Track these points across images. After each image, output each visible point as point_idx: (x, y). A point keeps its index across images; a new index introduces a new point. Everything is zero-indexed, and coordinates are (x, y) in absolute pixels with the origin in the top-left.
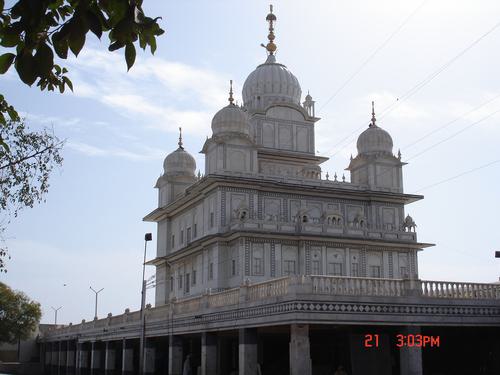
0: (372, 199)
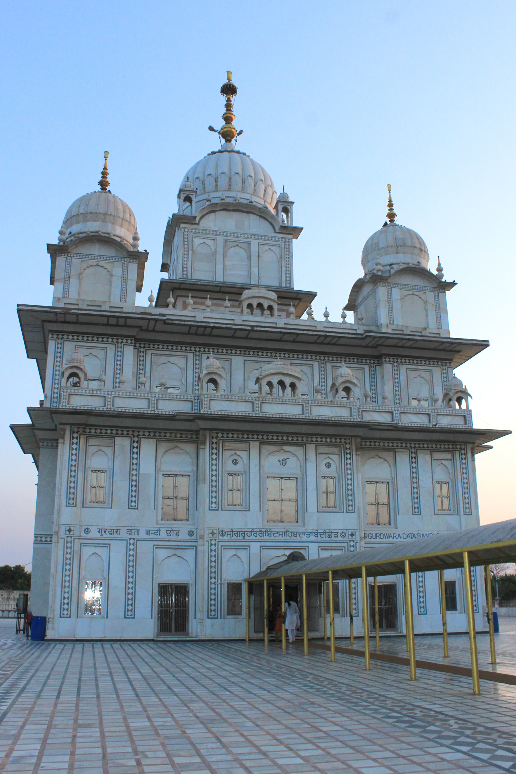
0: (385, 351)
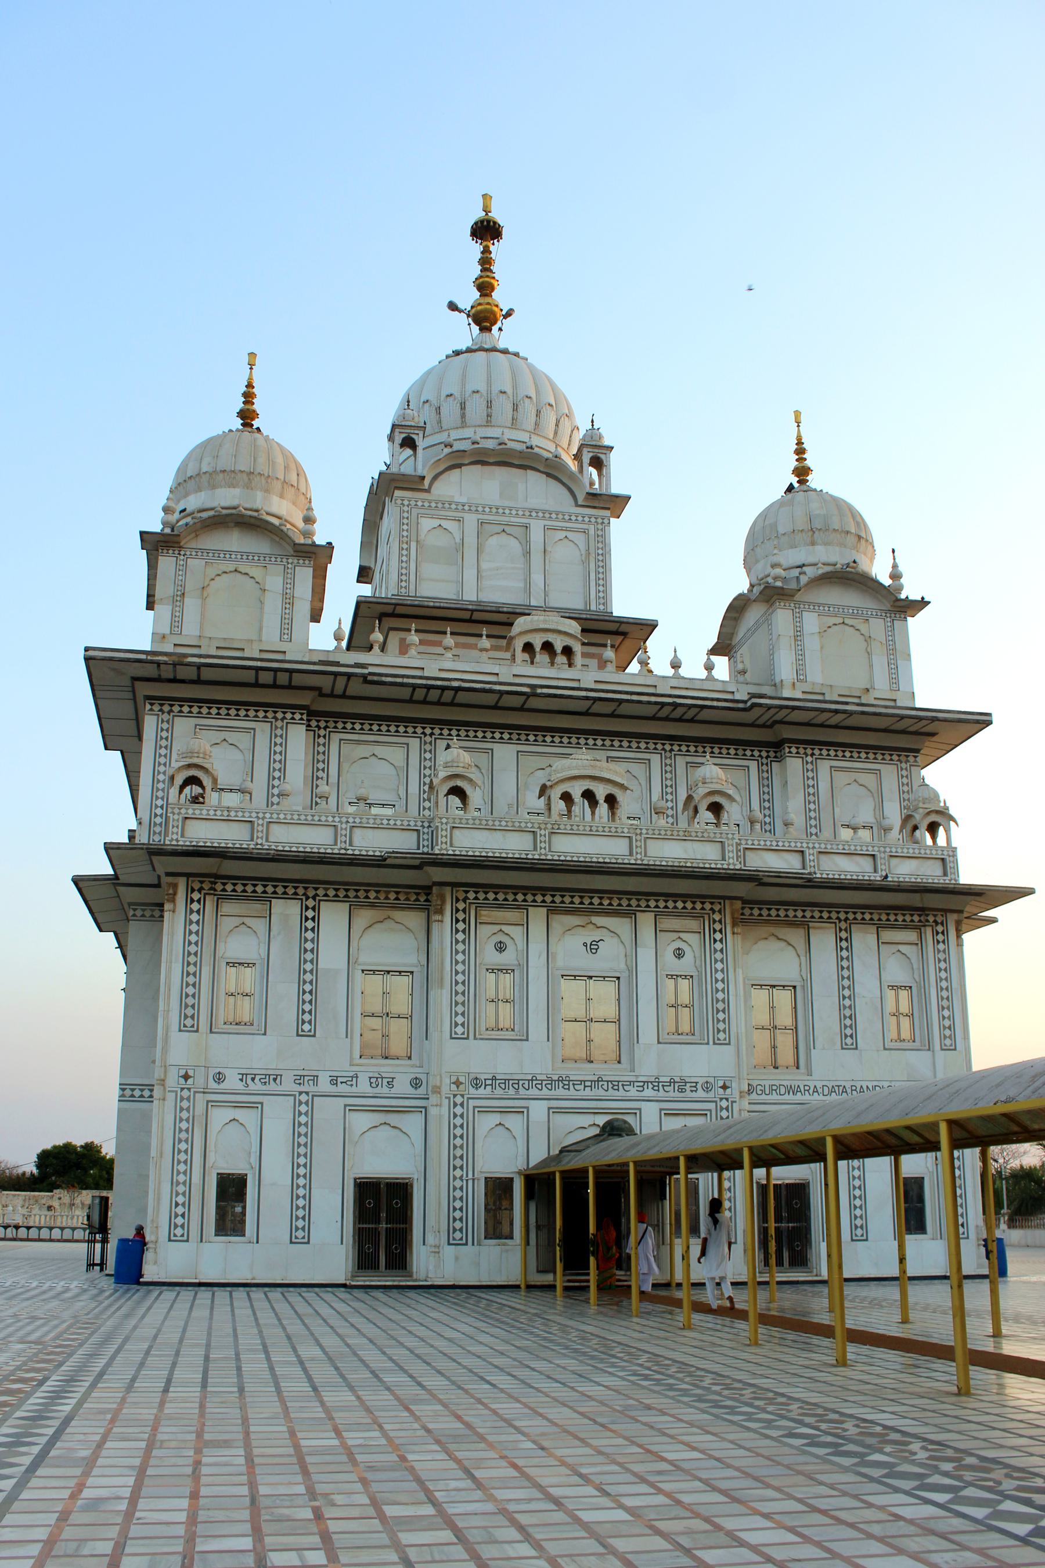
0: (787, 733)
